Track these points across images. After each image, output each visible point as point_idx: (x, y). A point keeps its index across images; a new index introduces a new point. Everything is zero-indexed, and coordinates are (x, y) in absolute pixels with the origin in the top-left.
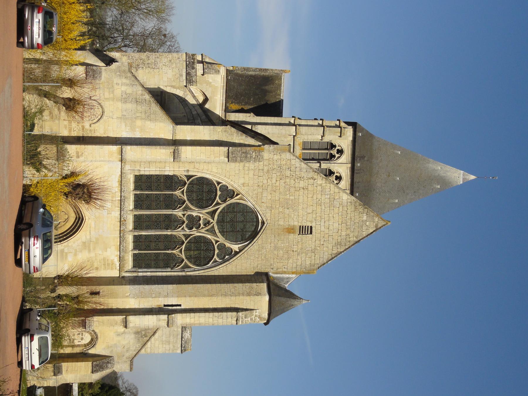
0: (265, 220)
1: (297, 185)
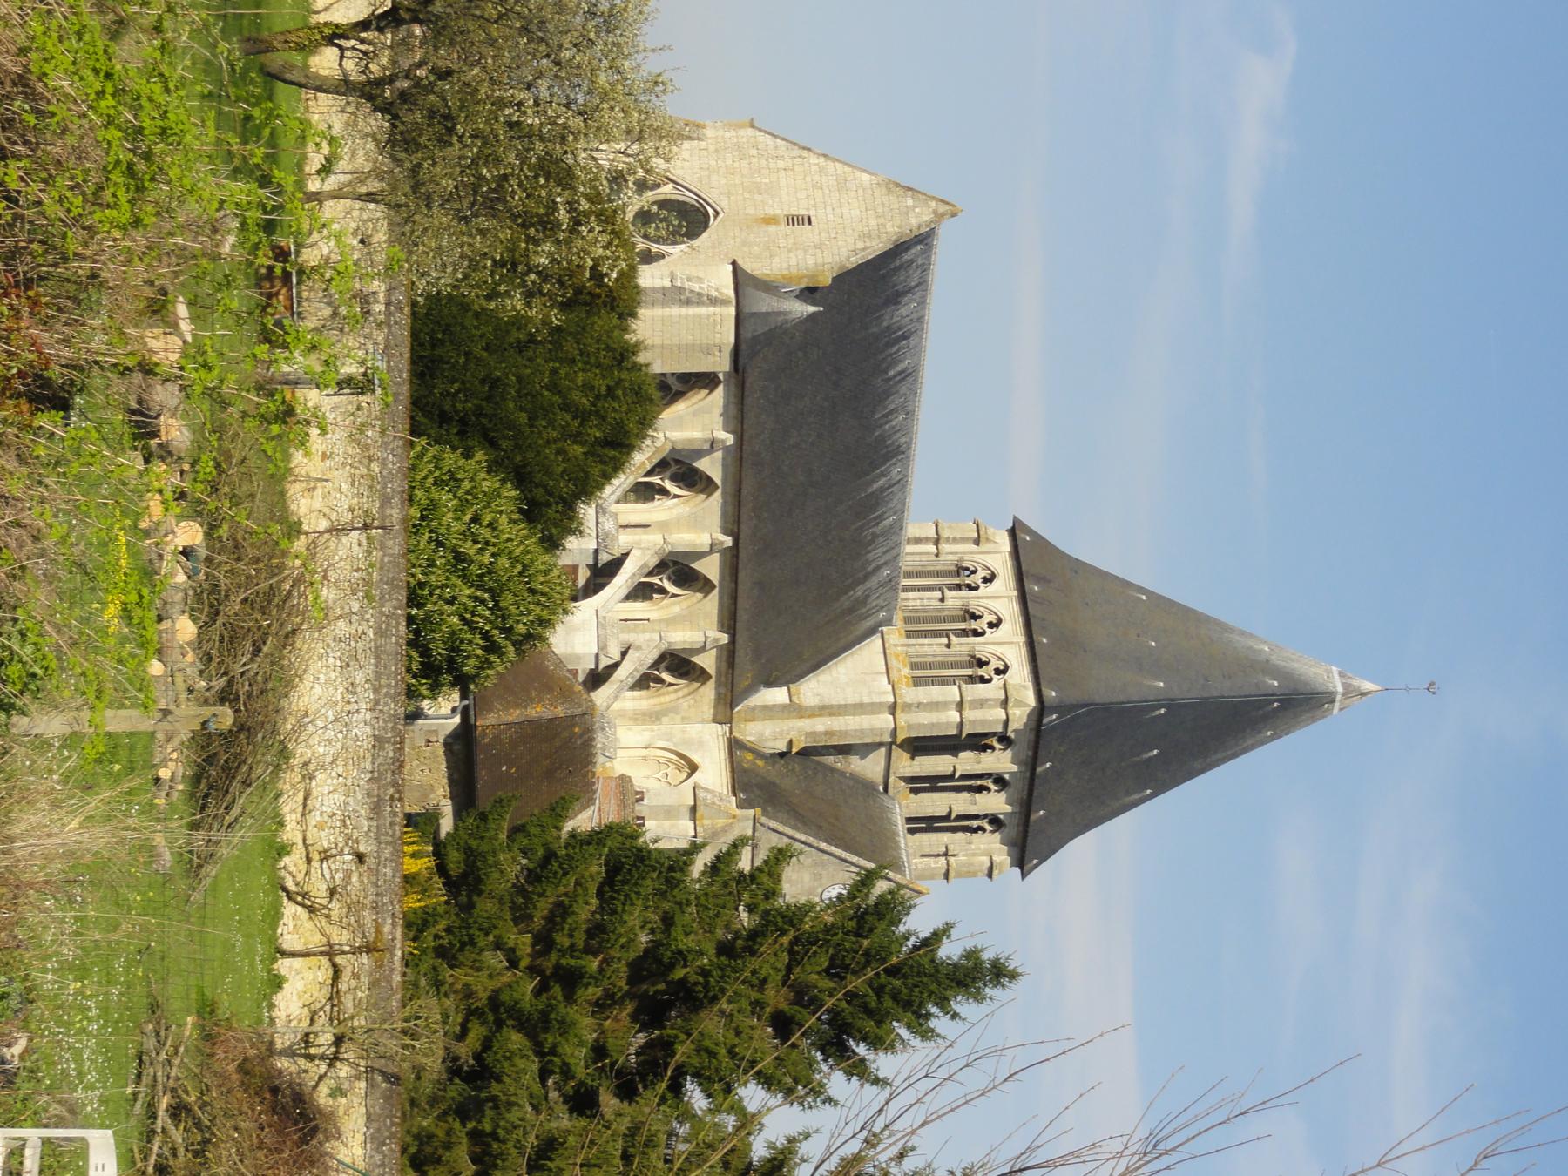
1: (772, 165)
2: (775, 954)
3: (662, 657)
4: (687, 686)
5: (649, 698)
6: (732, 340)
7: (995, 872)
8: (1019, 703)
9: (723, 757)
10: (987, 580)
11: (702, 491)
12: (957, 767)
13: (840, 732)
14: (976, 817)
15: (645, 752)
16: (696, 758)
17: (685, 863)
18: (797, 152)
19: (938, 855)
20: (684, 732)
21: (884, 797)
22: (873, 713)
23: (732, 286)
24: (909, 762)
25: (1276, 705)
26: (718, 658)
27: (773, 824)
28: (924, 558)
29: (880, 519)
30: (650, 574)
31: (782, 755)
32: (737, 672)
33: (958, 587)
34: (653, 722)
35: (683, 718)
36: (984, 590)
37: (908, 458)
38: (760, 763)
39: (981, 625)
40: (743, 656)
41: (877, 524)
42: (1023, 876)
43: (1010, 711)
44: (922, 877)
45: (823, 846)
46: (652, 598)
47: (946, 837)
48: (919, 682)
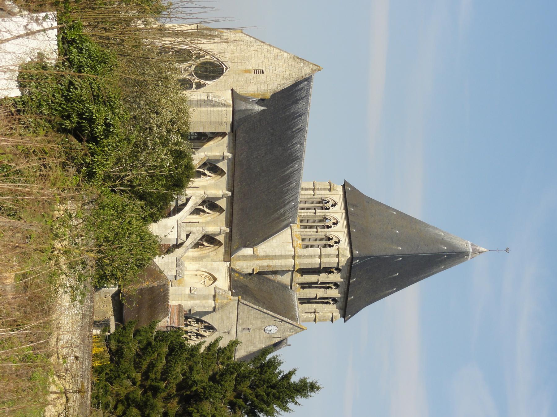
0: (228, 66)
1: (249, 49)
2: (230, 381)
3: (204, 236)
4: (213, 247)
5: (198, 251)
6: (231, 120)
7: (334, 320)
8: (344, 256)
9: (227, 275)
10: (333, 205)
11: (219, 175)
12: (319, 279)
13: (273, 266)
14: (327, 298)
15: (196, 273)
16: (216, 275)
17: (197, 348)
18: (259, 43)
19: (312, 313)
20: (212, 265)
21: (290, 291)
22: (286, 259)
23: (231, 99)
24: (300, 277)
25: (445, 256)
26: (225, 237)
27: (245, 302)
28: (309, 196)
29: (290, 184)
30: (200, 205)
31: (250, 274)
32: (233, 242)
33: (322, 208)
34: (200, 261)
35: (211, 259)
36: (332, 209)
37: (301, 161)
38: (241, 278)
39: (330, 223)
40: (235, 237)
41: (289, 186)
42: (345, 321)
43: (340, 259)
44: (304, 321)
45: (265, 311)
46: (199, 214)
47: (315, 306)
48: (305, 246)
